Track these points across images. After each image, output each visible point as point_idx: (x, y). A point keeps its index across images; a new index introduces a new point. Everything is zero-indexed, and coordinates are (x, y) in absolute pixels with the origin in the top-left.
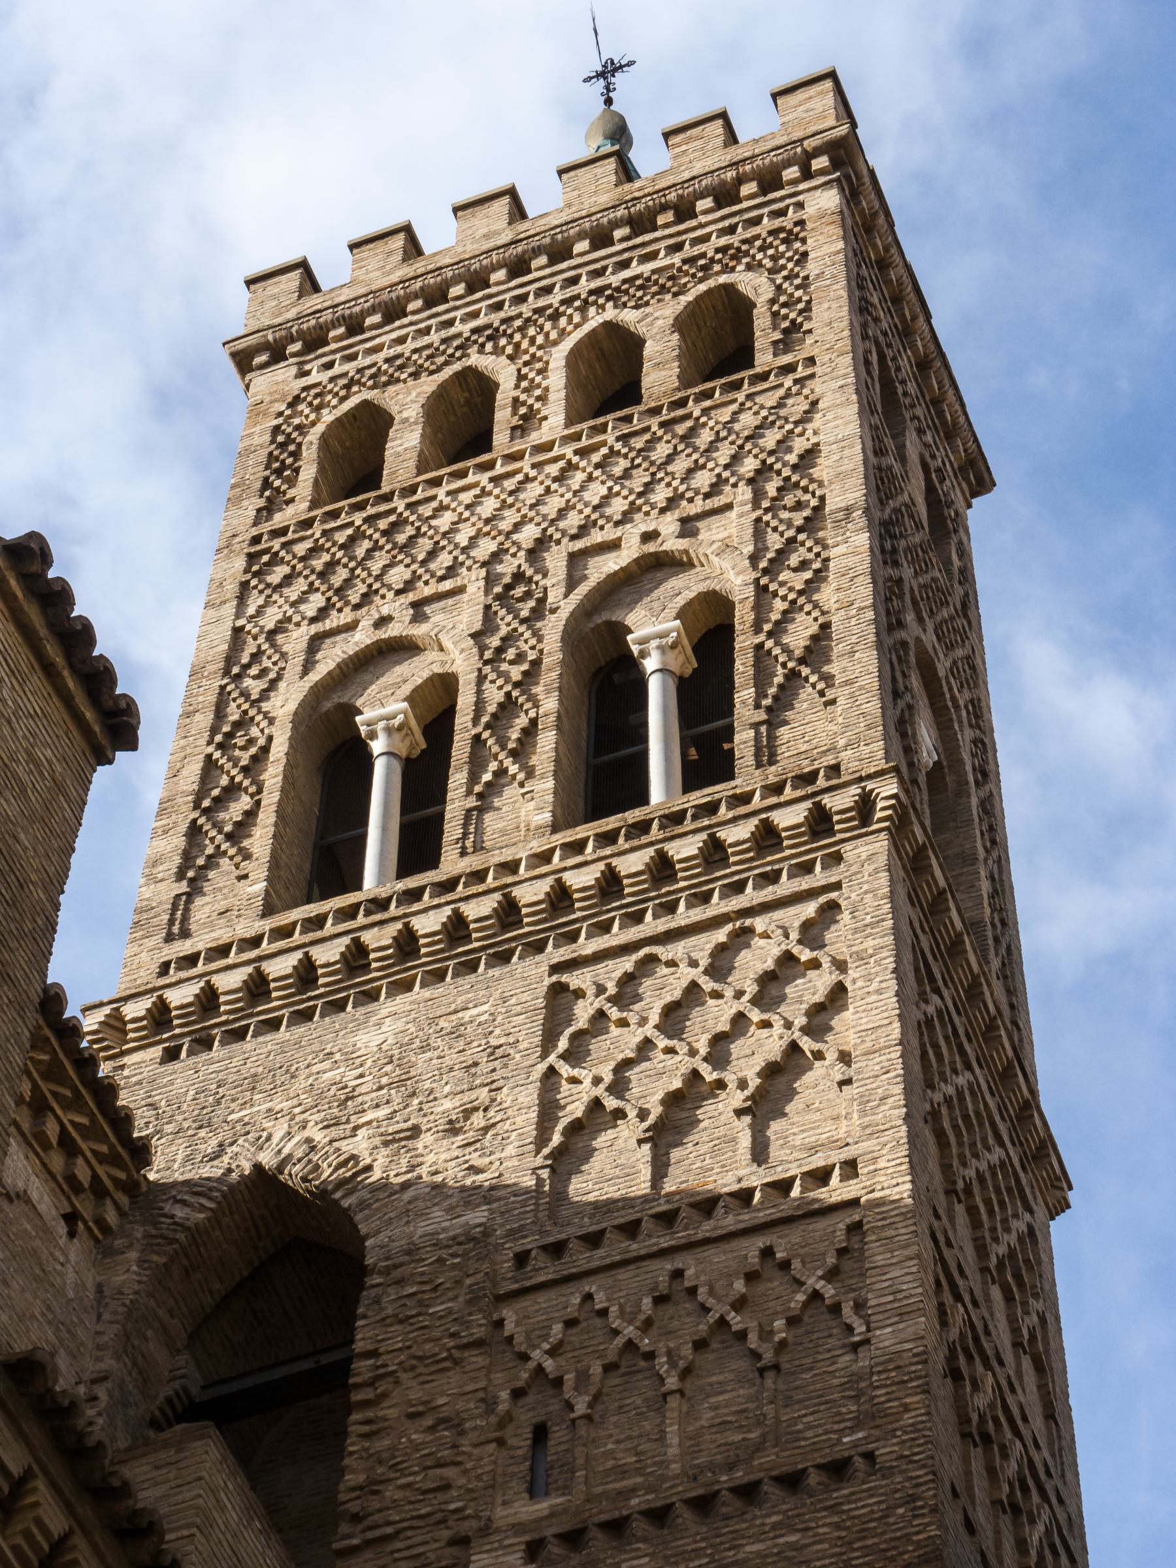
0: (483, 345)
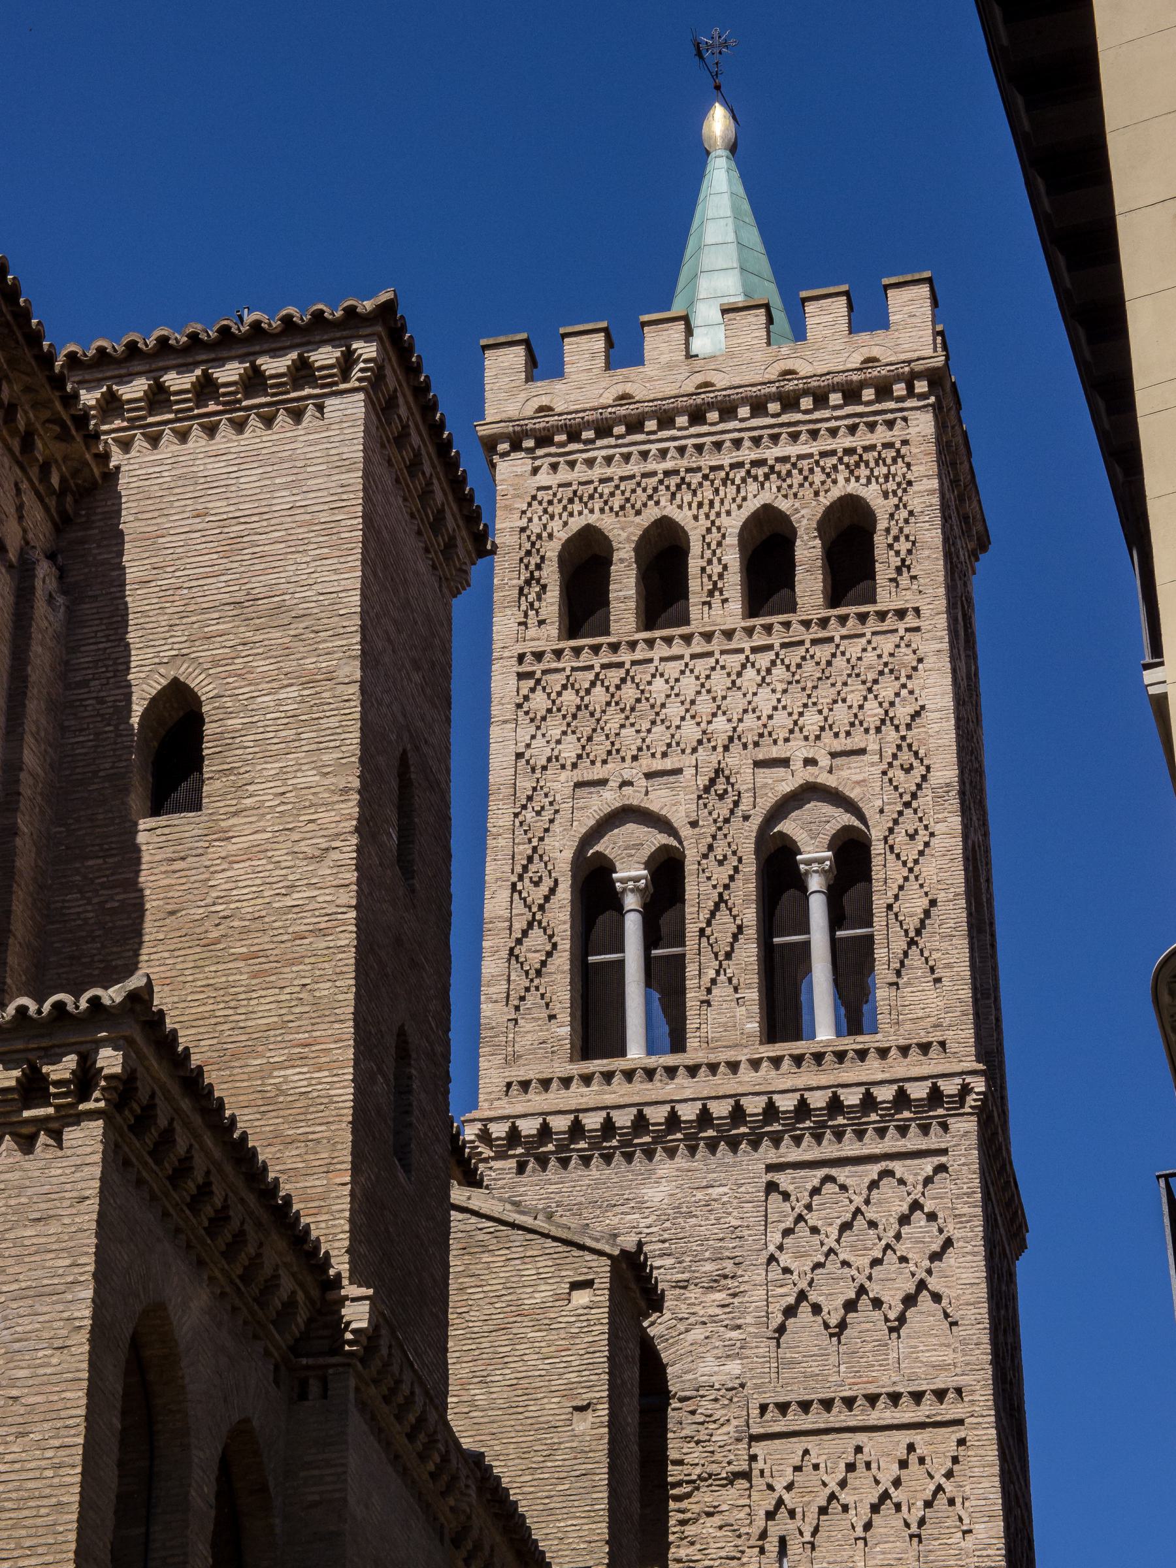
0: (673, 495)
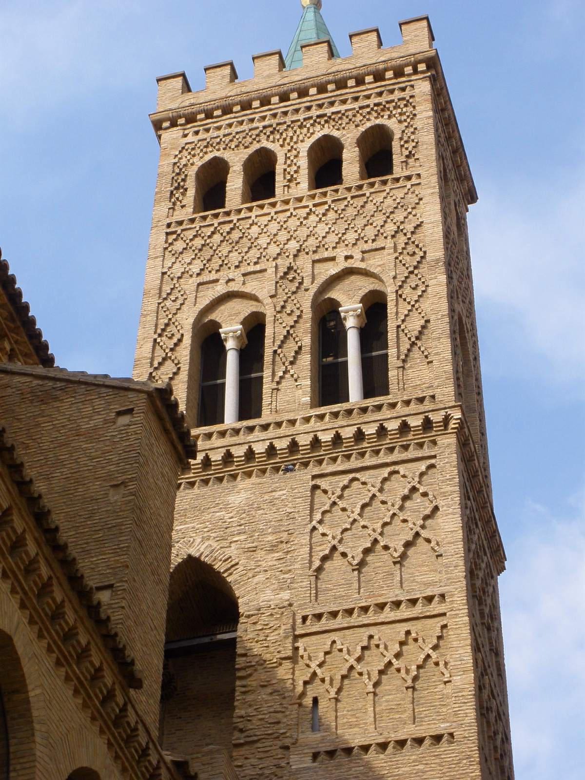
0: (268, 136)
